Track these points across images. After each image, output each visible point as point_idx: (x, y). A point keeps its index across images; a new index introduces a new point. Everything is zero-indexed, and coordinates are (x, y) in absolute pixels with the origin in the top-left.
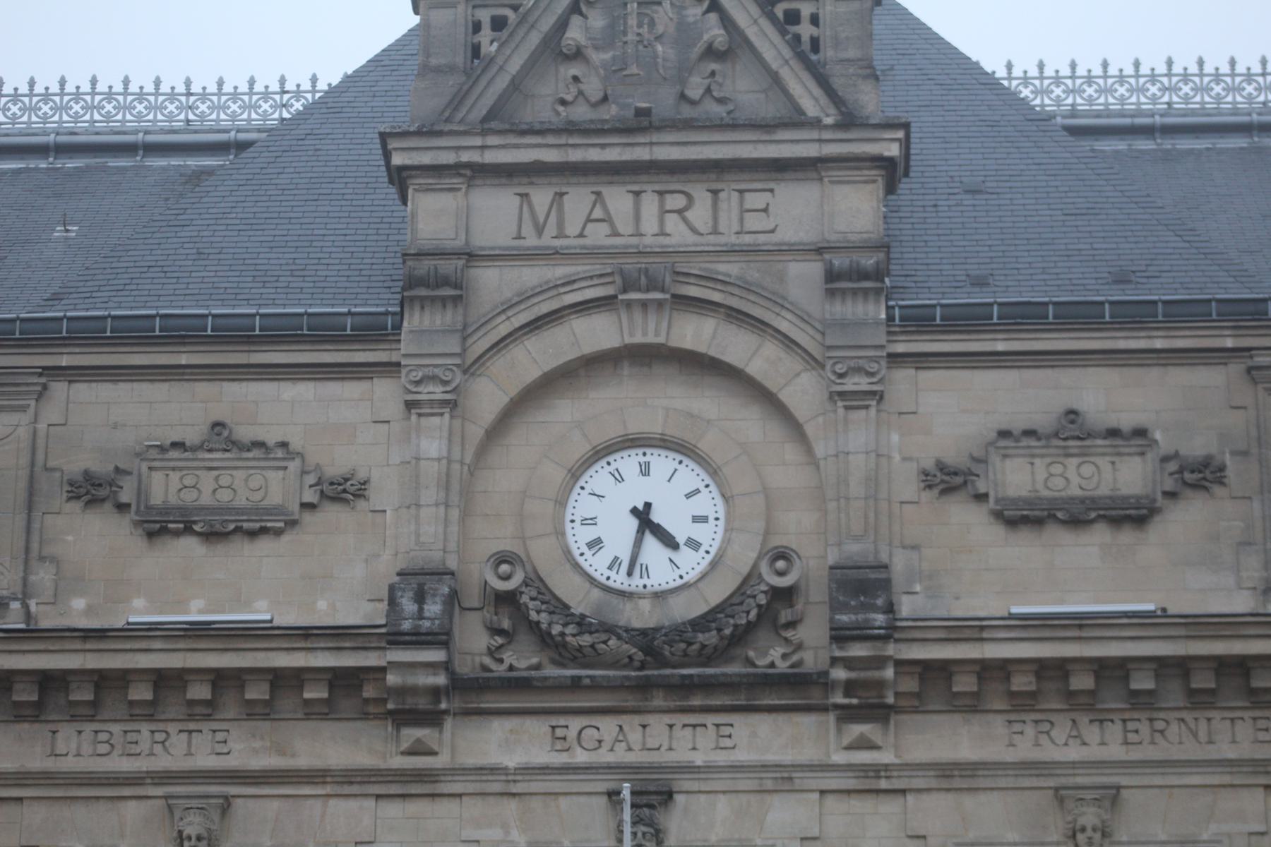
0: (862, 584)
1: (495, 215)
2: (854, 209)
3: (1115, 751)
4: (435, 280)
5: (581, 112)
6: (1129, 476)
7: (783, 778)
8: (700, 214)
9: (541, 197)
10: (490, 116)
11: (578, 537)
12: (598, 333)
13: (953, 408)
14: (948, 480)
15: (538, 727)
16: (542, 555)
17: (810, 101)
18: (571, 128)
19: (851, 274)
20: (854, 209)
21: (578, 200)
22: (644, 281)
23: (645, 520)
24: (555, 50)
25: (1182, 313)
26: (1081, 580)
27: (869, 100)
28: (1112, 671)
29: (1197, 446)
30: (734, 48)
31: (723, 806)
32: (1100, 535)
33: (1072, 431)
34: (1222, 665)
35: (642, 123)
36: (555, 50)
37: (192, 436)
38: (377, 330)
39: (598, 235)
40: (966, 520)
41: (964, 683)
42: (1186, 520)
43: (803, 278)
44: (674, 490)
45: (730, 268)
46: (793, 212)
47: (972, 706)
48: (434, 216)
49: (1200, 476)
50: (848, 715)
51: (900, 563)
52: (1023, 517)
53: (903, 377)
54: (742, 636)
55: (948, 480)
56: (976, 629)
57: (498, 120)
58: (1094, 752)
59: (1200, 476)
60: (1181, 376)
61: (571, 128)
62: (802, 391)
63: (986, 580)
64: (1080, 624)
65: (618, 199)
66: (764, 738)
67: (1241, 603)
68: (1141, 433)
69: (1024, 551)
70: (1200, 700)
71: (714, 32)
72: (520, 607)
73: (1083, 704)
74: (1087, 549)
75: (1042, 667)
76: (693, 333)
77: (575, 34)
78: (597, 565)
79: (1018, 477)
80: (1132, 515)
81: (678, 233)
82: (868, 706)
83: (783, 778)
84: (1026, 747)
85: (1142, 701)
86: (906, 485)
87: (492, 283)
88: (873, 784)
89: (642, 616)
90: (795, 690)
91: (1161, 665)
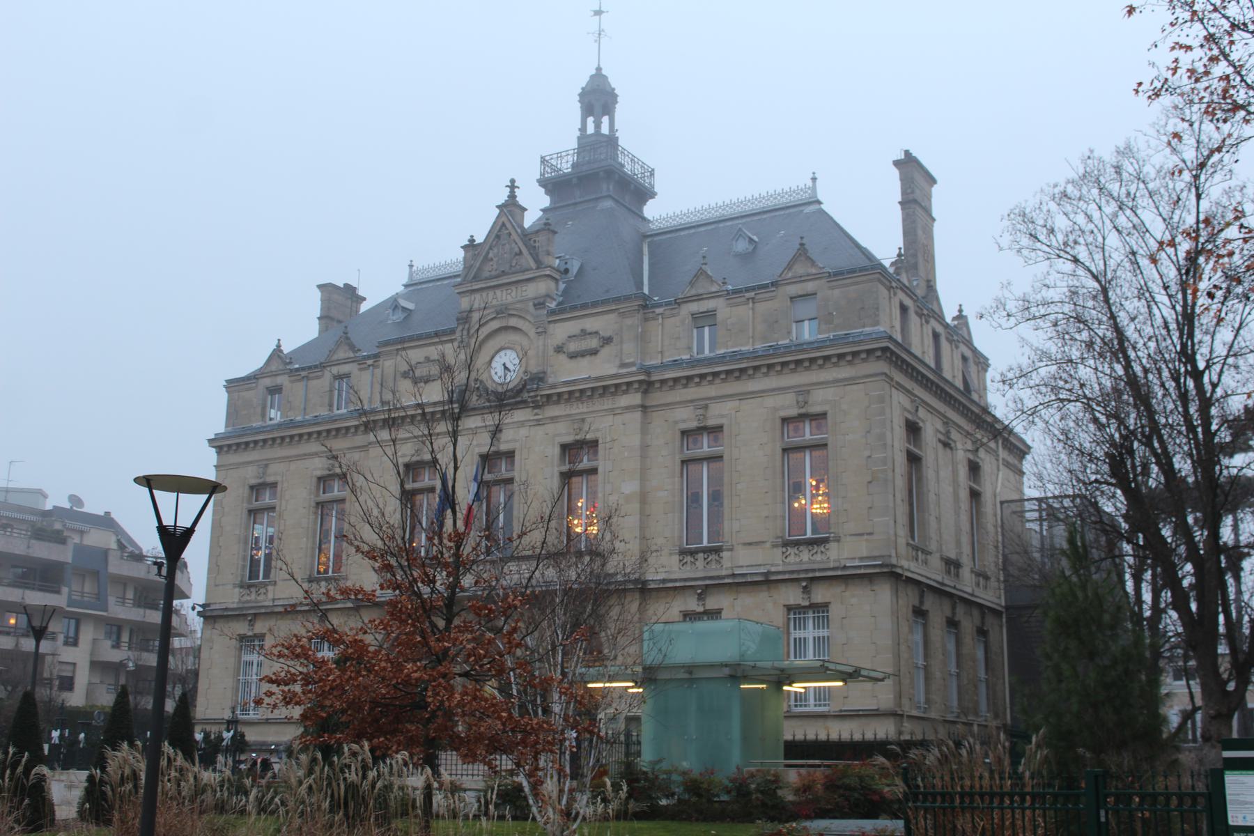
0: (539, 378)
1: (478, 301)
2: (542, 287)
3: (585, 410)
4: (464, 319)
5: (494, 273)
6: (593, 343)
7: (522, 424)
8: (514, 294)
9: (484, 294)
10: (474, 277)
11: (493, 372)
12: (495, 325)
13: (561, 331)
14: (559, 349)
15: (479, 418)
16: (484, 377)
17: (533, 265)
18: (487, 279)
19: (539, 305)
20: (542, 287)
21: (491, 293)
22: (503, 311)
23: (504, 366)
24: (486, 259)
25: (604, 302)
26: (583, 370)
27: (548, 260)
28: (582, 391)
29: (607, 334)
30: (521, 253)
31: (511, 432)
32: (588, 358)
33: (584, 333)
34: (605, 388)
35: (504, 273)
36: (486, 259)
37: (422, 360)
38: (453, 331)
39: (494, 302)
40: (562, 358)
41: (555, 398)
42: (605, 352)
43: (531, 308)
44: (509, 358)
45: (518, 306)
46: (532, 290)
47: (558, 402)
48: (465, 303)
49: (607, 341)
50: (534, 408)
51: (549, 370)
52: (573, 356)
53: (552, 325)
54: (520, 391)
55: (559, 349)
56: (553, 386)
57: (476, 278)
58: (581, 410)
59: (607, 341)
60: (606, 317)
61: (487, 279)
62: (532, 333)
63: (567, 372)
64: (574, 382)
65: (498, 292)
66: (520, 415)
67: (613, 371)
68: (596, 333)
69: (573, 364)
70: (602, 395)
71: (517, 250)
72: (483, 390)
73: (579, 399)
74: (584, 362)
75: (570, 393)
76: (513, 322)
77: (491, 255)
78: (496, 378)
79: (573, 347)
80: (594, 352)
81: (510, 299)
82: (537, 406)
83: (522, 424)
84: (568, 412)
85: (590, 397)
86: (551, 351)
87: (476, 316)
88: (539, 423)
89: (500, 390)
90: (523, 404)
91: (593, 389)
